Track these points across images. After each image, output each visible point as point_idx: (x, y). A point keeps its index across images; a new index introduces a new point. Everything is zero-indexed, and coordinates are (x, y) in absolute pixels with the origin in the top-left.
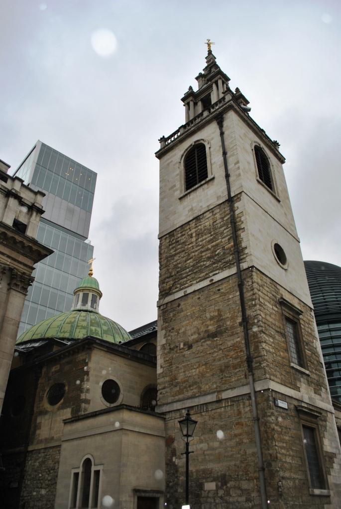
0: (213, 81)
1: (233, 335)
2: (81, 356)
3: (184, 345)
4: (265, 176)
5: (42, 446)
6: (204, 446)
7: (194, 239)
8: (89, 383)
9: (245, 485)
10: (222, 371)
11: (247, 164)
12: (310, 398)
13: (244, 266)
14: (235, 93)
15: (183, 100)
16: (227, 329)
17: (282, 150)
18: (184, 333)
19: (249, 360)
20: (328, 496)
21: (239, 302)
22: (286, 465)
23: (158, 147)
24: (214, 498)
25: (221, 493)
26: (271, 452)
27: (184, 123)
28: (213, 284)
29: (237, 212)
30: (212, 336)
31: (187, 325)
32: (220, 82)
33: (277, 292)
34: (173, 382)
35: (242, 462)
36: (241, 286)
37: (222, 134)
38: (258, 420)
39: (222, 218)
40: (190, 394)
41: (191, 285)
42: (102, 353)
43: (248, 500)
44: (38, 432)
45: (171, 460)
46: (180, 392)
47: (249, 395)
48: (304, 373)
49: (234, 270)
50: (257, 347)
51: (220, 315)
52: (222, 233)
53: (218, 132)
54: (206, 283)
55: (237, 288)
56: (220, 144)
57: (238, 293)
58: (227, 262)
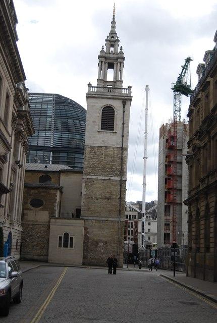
5: (26, 223)
9: (113, 245)
10: (109, 211)
18: (95, 193)
25: (104, 246)
28: (110, 179)
29: (124, 155)
30: (108, 199)
34: (89, 209)
36: (121, 186)
37: (124, 112)
45: (86, 235)
49: (119, 179)
52: (116, 161)
56: (122, 116)
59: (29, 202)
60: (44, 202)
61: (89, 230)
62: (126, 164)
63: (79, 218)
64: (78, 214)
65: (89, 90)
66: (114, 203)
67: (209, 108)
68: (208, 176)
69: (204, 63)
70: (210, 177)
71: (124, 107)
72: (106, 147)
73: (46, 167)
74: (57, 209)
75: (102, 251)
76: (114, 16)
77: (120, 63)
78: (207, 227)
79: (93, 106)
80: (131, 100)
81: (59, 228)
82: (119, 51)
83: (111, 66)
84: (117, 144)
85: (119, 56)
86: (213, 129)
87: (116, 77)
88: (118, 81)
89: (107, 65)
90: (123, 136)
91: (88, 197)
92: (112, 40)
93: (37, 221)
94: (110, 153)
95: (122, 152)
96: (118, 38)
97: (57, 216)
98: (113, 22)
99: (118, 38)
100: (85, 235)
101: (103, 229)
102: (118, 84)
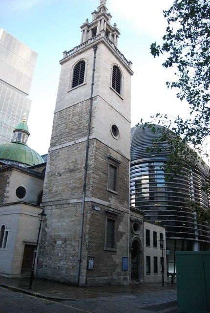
0: (99, 19)
2: (6, 174)
4: (116, 84)
6: (59, 224)
7: (71, 117)
8: (9, 188)
9: (73, 243)
11: (107, 76)
12: (115, 206)
13: (91, 137)
14: (113, 26)
15: (82, 27)
16: (78, 169)
17: (133, 68)
19: (85, 186)
20: (116, 252)
21: (85, 156)
22: (93, 236)
23: (62, 57)
24: (60, 248)
25: (63, 246)
26: (86, 230)
27: (79, 43)
29: (93, 107)
30: (71, 171)
31: (61, 164)
32: (103, 21)
33: (108, 152)
34: (50, 192)
35: (74, 233)
36: (88, 147)
37: (95, 57)
38: (83, 215)
42: (18, 173)
43: (74, 250)
46: (53, 197)
48: (115, 194)
49: (86, 139)
53: (93, 56)
54: (73, 143)
55: (86, 148)
58: (84, 134)
71: (95, 53)
79: (65, 70)
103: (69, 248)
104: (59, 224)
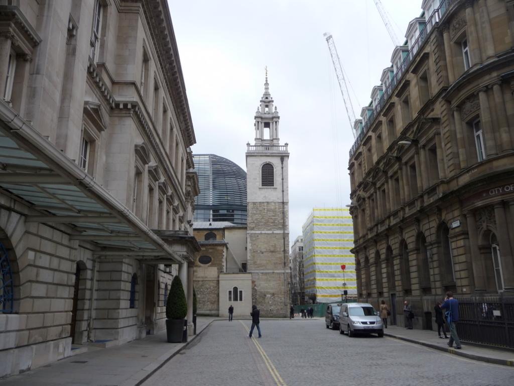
1: (280, 254)
3: (260, 251)
6: (267, 285)
9: (280, 296)
28: (273, 233)
29: (285, 210)
30: (272, 252)
34: (255, 263)
36: (284, 239)
37: (282, 168)
39: (279, 209)
40: (262, 268)
41: (264, 230)
44: (195, 274)
47: (284, 273)
50: (287, 260)
51: (275, 246)
52: (278, 215)
55: (282, 238)
57: (283, 241)
59: (198, 259)
60: (212, 259)
61: (256, 283)
62: (288, 218)
63: (245, 271)
64: (244, 268)
65: (249, 149)
66: (279, 256)
67: (372, 161)
68: (377, 225)
69: (361, 118)
70: (379, 226)
71: (282, 163)
72: (268, 203)
73: (210, 224)
74: (224, 264)
75: (270, 303)
76: (266, 78)
77: (276, 122)
78: (379, 273)
80: (288, 156)
81: (228, 283)
82: (274, 111)
83: (267, 125)
84: (278, 199)
85: (274, 115)
86: (379, 180)
87: (271, 135)
88: (274, 139)
89: (263, 124)
90: (283, 191)
91: (254, 252)
92: (267, 101)
93: (206, 277)
94: (272, 208)
95: (283, 207)
96: (272, 98)
97: (225, 270)
98: (267, 84)
99: (272, 98)
100: (253, 289)
101: (269, 281)
102: (275, 141)
103: (276, 299)
104: (267, 285)
